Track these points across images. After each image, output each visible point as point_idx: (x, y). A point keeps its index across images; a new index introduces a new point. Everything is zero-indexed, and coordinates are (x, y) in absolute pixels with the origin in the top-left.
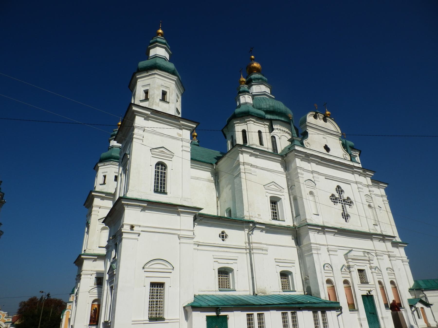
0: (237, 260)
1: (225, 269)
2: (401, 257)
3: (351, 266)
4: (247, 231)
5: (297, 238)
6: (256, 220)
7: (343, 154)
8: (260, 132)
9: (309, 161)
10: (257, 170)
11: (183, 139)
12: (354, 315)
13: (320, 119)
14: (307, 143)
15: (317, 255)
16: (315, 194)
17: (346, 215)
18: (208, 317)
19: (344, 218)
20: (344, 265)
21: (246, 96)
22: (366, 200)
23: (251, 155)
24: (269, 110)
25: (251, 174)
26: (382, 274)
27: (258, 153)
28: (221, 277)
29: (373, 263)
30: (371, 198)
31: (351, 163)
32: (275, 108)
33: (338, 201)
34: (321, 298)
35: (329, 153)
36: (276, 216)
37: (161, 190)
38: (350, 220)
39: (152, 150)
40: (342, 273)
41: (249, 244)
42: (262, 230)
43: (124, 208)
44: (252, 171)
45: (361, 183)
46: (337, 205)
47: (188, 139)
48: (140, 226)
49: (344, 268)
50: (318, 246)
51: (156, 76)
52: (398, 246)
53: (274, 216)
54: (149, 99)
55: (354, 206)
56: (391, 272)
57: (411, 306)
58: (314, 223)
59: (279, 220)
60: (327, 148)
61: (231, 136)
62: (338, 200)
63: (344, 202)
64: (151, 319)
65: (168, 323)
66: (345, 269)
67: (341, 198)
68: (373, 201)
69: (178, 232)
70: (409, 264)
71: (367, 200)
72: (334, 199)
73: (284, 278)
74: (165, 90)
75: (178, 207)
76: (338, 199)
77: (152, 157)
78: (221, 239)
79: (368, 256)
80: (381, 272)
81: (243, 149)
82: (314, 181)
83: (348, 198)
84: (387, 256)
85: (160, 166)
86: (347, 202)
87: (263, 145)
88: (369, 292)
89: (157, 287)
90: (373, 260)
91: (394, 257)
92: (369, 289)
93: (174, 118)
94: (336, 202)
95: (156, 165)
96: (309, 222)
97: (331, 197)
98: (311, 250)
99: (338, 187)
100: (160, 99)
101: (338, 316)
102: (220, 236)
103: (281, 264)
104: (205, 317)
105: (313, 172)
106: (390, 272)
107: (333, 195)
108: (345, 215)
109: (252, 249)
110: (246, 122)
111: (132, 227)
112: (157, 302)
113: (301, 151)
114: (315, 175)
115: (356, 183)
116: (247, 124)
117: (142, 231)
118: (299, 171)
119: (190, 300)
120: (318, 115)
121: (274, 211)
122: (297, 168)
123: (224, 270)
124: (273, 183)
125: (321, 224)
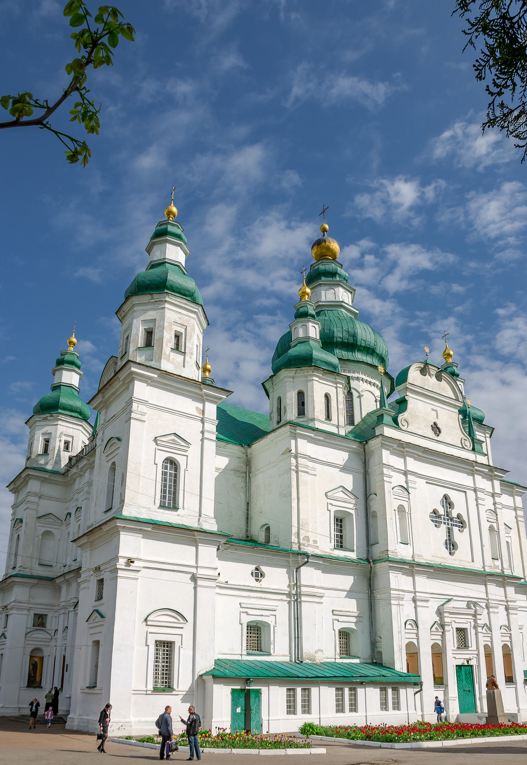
1: (257, 624)
3: (446, 624)
5: (370, 578)
15: (396, 606)
20: (436, 622)
22: (487, 518)
25: (308, 473)
26: (492, 634)
29: (481, 619)
31: (471, 456)
33: (443, 521)
34: (395, 670)
37: (169, 504)
40: (432, 633)
42: (317, 567)
44: (309, 468)
47: (212, 418)
48: (140, 560)
49: (436, 626)
50: (401, 593)
56: (506, 632)
60: (436, 429)
71: (488, 519)
76: (442, 517)
78: (254, 578)
80: (491, 633)
90: (481, 614)
91: (516, 609)
92: (468, 657)
99: (446, 497)
101: (415, 694)
102: (252, 574)
107: (435, 512)
111: (130, 561)
117: (144, 567)
118: (385, 471)
120: (429, 368)
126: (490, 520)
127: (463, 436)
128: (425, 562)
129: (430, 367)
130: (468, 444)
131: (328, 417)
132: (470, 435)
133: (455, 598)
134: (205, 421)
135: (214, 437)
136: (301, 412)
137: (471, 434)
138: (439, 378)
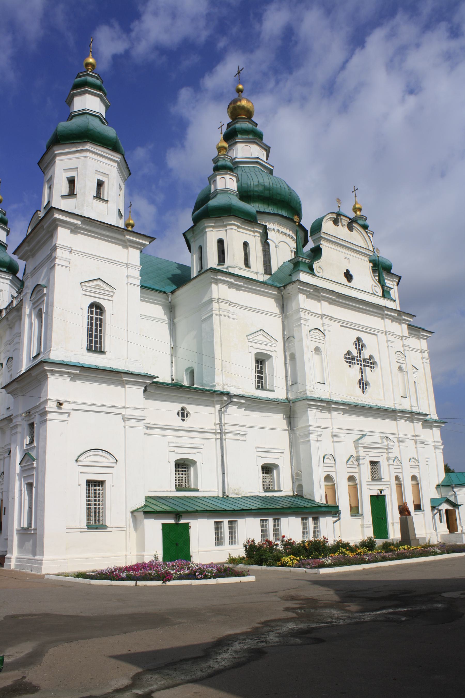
0: (202, 448)
1: (184, 462)
2: (434, 442)
3: (360, 457)
4: (218, 407)
5: (290, 416)
6: (233, 391)
7: (372, 286)
8: (246, 244)
9: (319, 299)
10: (238, 311)
11: (128, 265)
12: (357, 521)
13: (342, 226)
14: (319, 267)
15: (315, 442)
16: (323, 352)
17: (364, 382)
18: (164, 525)
19: (361, 388)
21: (228, 177)
23: (231, 285)
24: (262, 194)
25: (229, 317)
26: (402, 466)
27: (242, 284)
28: (177, 473)
29: (392, 453)
30: (404, 357)
32: (273, 193)
33: (356, 362)
35: (352, 284)
36: (262, 383)
37: (96, 347)
38: (369, 390)
39: (83, 284)
41: (221, 425)
42: (240, 406)
43: (47, 375)
44: (230, 313)
45: (392, 334)
46: (353, 367)
48: (69, 402)
49: (352, 459)
50: (319, 429)
51: (88, 154)
52: (433, 426)
53: (258, 382)
54: (76, 194)
55: (377, 369)
57: (433, 508)
58: (317, 395)
59: (266, 390)
60: (348, 276)
61: (199, 245)
62: (356, 360)
63: (364, 362)
64: (89, 527)
65: (111, 531)
66: (352, 461)
67: (360, 357)
68: (406, 361)
69: (123, 412)
70: (443, 451)
72: (349, 359)
73: (267, 473)
74: (101, 178)
75: (123, 375)
76: (356, 358)
77: (83, 294)
78: (180, 418)
79: (386, 443)
80: (401, 465)
81: (219, 277)
82: (324, 330)
83: (371, 357)
84: (413, 441)
85: (94, 308)
86: (368, 363)
87: (250, 267)
88: (381, 492)
89: (95, 486)
90: (392, 448)
91: (423, 443)
92: (381, 487)
93: (117, 230)
94: (352, 362)
95: (89, 308)
96: (309, 394)
97: (346, 354)
98: (308, 435)
99: (359, 339)
100: (94, 196)
101: (334, 523)
102: (178, 414)
103: (264, 455)
104: (161, 526)
105: (322, 316)
106: (413, 463)
107: (349, 353)
108: (363, 383)
109: (225, 433)
110: (225, 226)
111: (60, 404)
112: (95, 505)
113: (307, 283)
114: (326, 321)
115: (386, 333)
116: (226, 230)
117: (73, 410)
119: (141, 503)
120: (341, 219)
121: (260, 375)
122: (299, 310)
123: (183, 462)
124: (262, 331)
125: (325, 396)
126: (399, 361)
127: (374, 283)
128: (340, 400)
129: (342, 217)
130: (379, 291)
131: (247, 264)
132: (379, 282)
133: (368, 434)
134: (129, 266)
135: (138, 282)
136: (222, 258)
137: (381, 282)
138: (350, 228)
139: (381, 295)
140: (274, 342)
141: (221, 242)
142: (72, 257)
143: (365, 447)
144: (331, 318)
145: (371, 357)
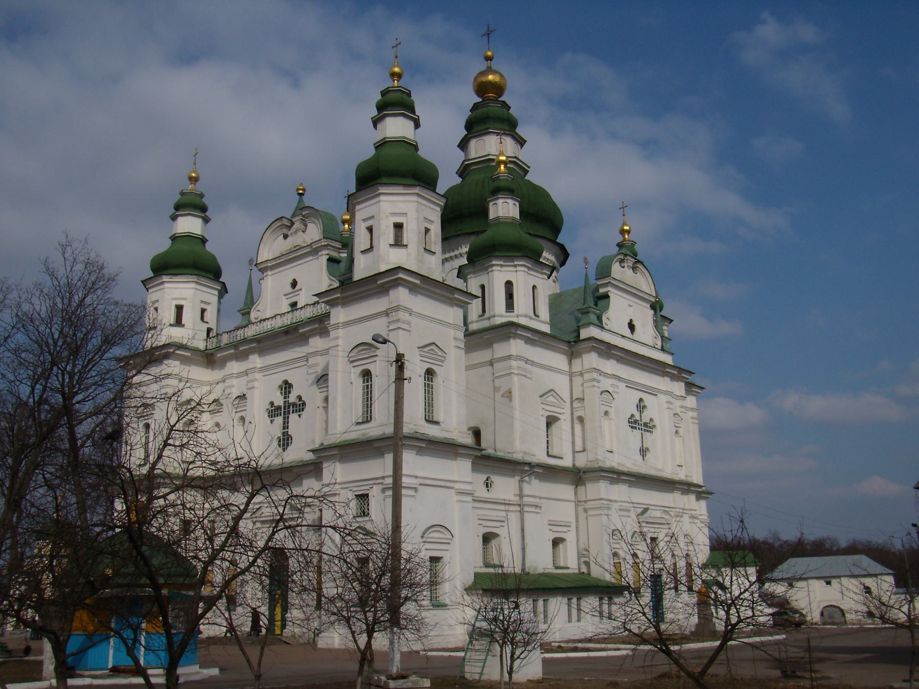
4: (517, 478)
27: (537, 339)
49: (636, 535)
60: (631, 327)
69: (457, 486)
72: (632, 422)
82: (613, 392)
99: (641, 400)
117: (420, 484)
133: (651, 507)
139: (660, 348)
140: (563, 403)
141: (509, 284)
142: (414, 320)
143: (647, 523)
144: (619, 378)
145: (651, 420)
